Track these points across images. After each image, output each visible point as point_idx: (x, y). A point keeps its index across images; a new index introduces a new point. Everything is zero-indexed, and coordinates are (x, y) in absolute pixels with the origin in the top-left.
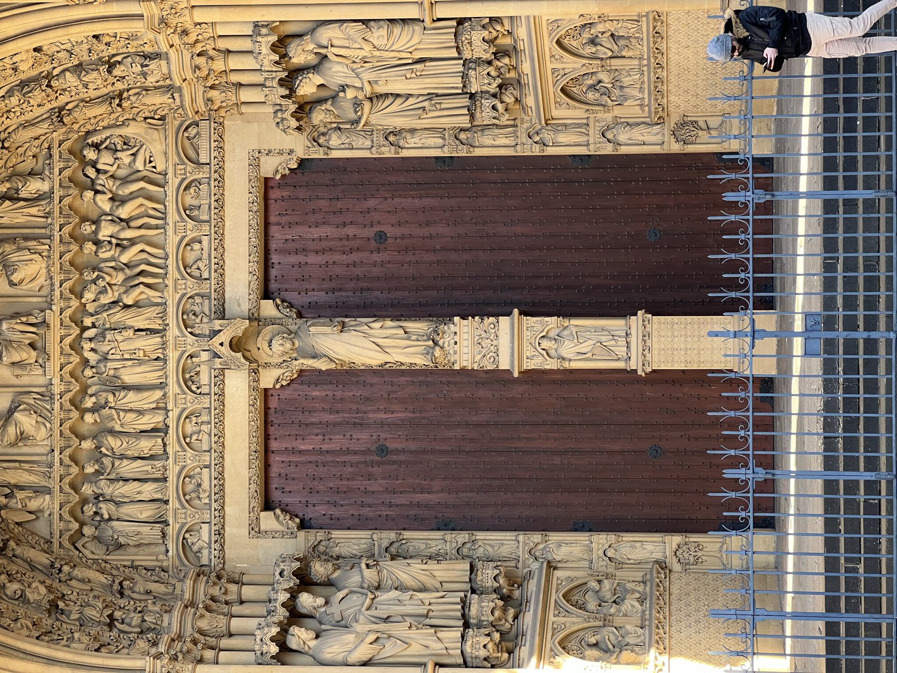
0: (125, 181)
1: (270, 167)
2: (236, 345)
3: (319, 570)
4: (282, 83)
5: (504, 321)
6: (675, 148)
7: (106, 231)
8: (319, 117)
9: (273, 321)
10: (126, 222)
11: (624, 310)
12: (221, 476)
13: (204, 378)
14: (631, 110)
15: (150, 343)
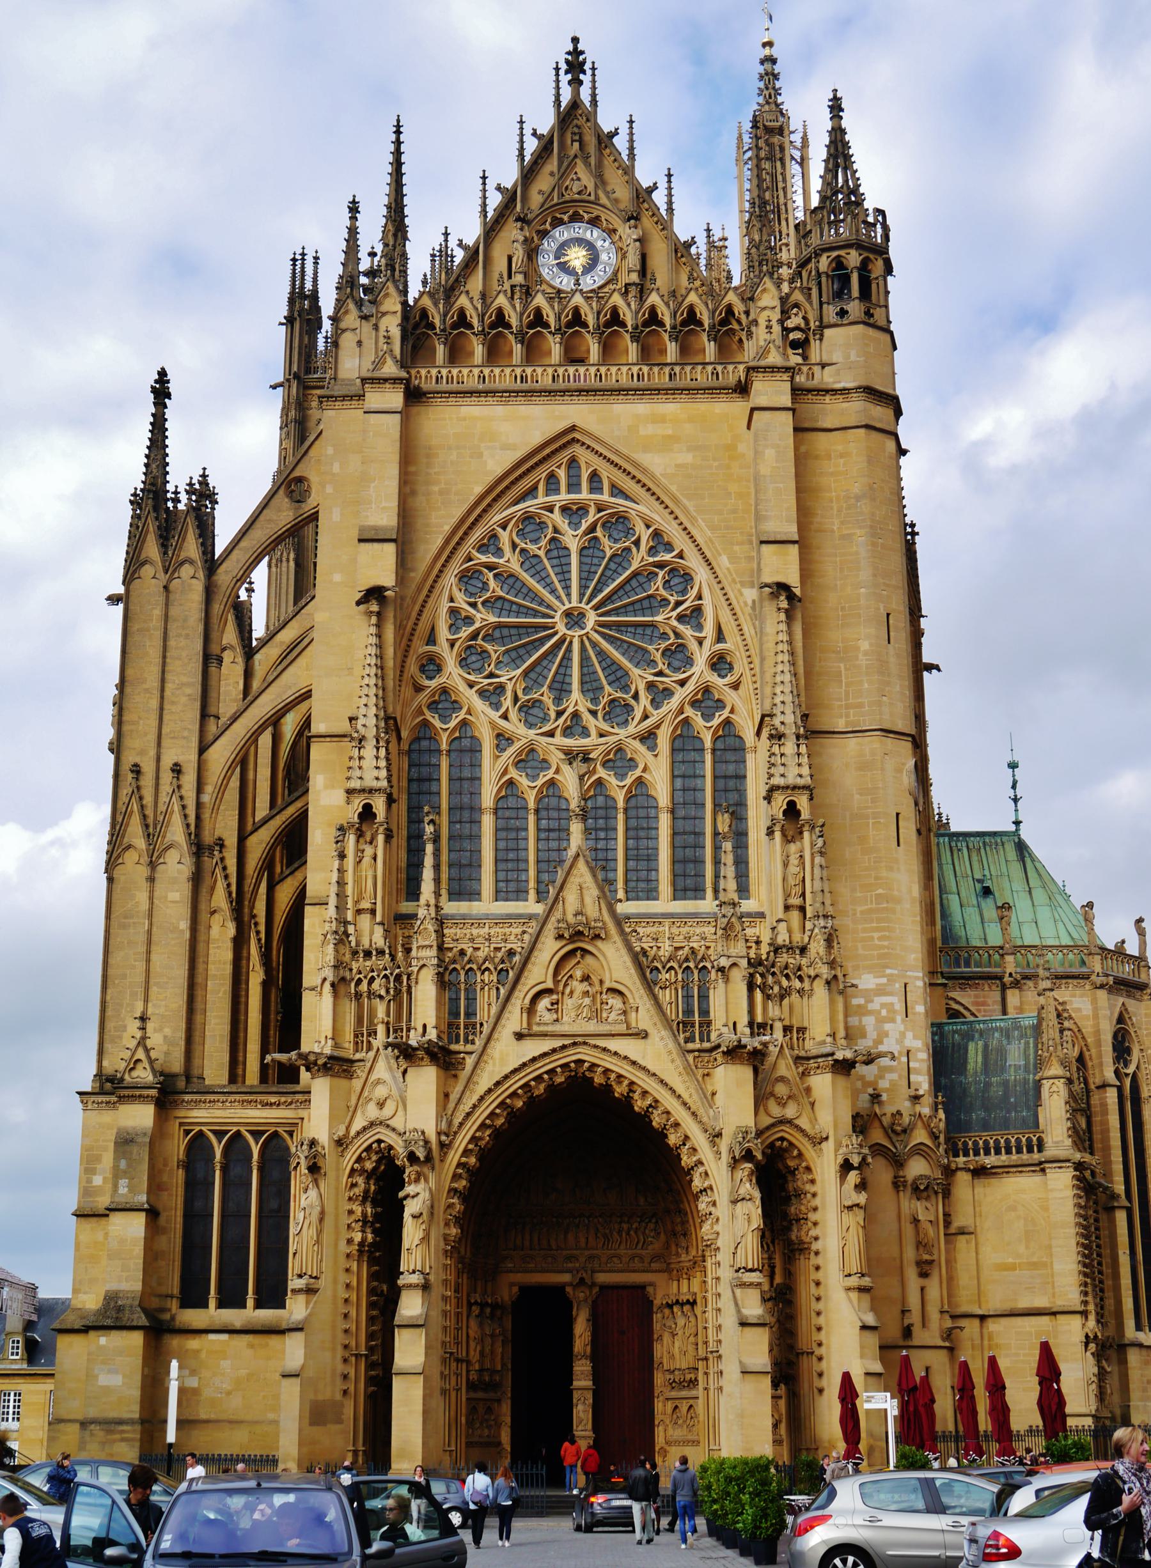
0: (644, 1233)
1: (650, 1289)
2: (582, 1280)
3: (499, 1313)
4: (677, 1301)
5: (591, 1383)
6: (657, 1449)
7: (625, 1226)
8: (667, 1311)
9: (591, 1292)
10: (628, 1234)
11: (595, 1428)
12: (532, 1272)
13: (570, 1265)
14: (670, 1432)
15: (583, 1245)
